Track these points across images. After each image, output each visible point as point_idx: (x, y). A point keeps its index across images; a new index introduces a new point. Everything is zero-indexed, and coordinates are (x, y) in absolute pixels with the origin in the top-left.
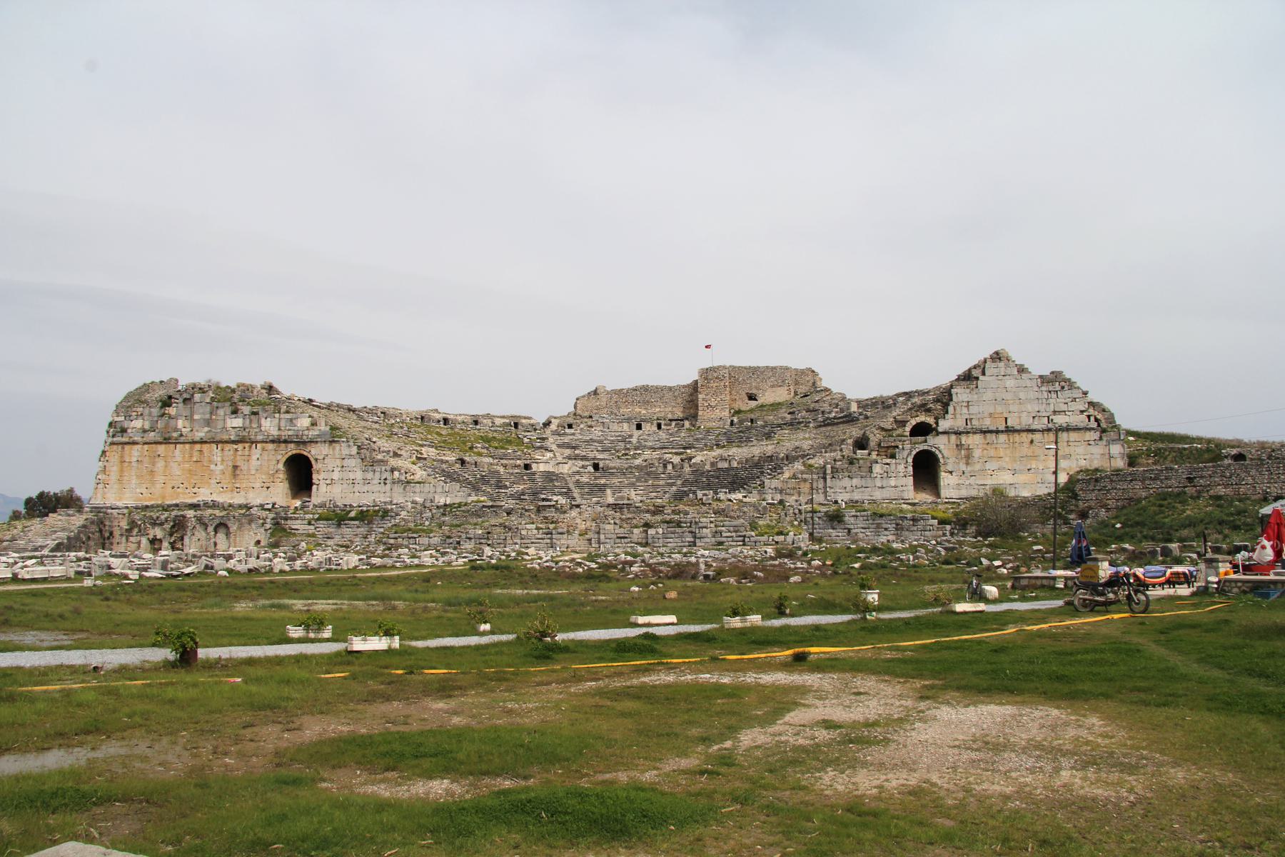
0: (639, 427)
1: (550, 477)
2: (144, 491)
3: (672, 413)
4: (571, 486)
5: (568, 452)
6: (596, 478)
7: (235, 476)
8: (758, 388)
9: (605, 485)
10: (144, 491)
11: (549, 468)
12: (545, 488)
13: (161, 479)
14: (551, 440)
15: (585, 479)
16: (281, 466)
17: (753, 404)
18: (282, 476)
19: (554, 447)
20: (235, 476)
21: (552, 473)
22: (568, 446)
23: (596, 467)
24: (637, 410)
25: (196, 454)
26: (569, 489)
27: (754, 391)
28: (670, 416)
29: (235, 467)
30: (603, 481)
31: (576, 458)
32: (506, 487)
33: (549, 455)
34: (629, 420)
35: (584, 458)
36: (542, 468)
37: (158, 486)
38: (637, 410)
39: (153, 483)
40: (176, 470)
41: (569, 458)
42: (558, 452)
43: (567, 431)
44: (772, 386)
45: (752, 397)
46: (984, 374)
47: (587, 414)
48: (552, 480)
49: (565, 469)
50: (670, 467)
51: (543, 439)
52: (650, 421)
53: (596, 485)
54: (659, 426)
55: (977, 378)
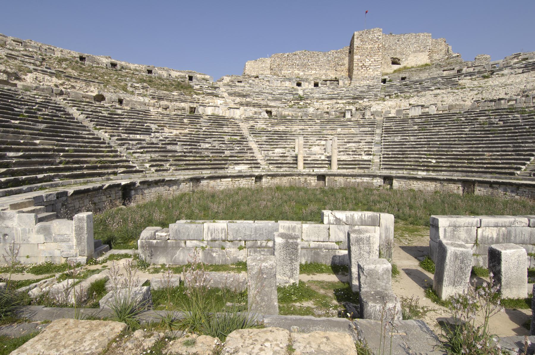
0: (299, 85)
1: (218, 121)
3: (326, 75)
4: (245, 132)
5: (238, 100)
6: (273, 125)
8: (402, 54)
9: (285, 133)
11: (220, 112)
12: (211, 136)
14: (222, 89)
15: (260, 125)
17: (396, 67)
19: (225, 95)
21: (224, 118)
22: (240, 95)
23: (269, 113)
24: (296, 72)
26: (243, 137)
27: (398, 56)
28: (324, 77)
30: (281, 128)
31: (248, 104)
32: (148, 131)
33: (219, 101)
34: (290, 80)
35: (259, 106)
36: (209, 111)
38: (296, 72)
41: (242, 104)
42: (230, 100)
43: (237, 84)
44: (415, 52)
45: (395, 62)
47: (254, 74)
48: (221, 126)
49: (238, 114)
50: (348, 116)
51: (216, 88)
52: (306, 80)
53: (276, 132)
54: (316, 85)
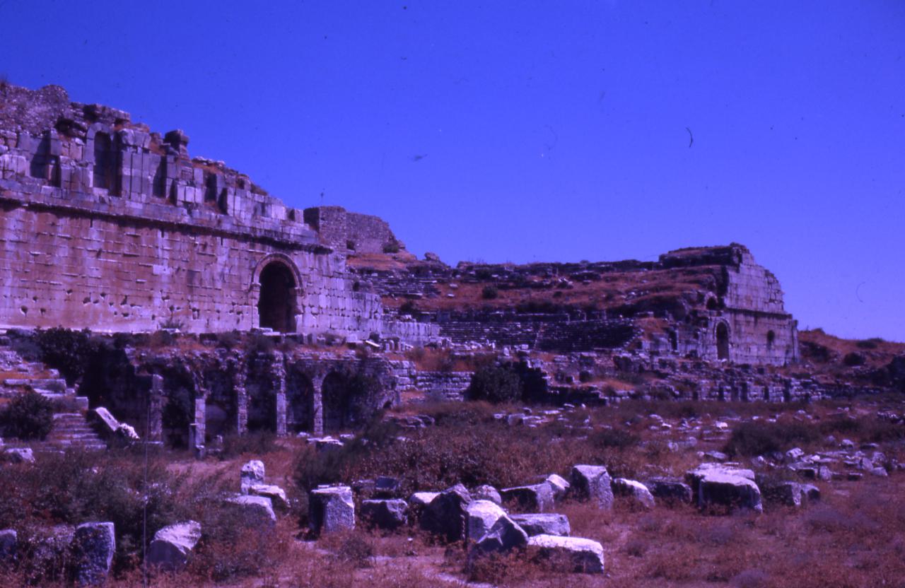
2: (30, 304)
7: (191, 289)
8: (355, 236)
10: (30, 304)
13: (61, 281)
16: (257, 281)
18: (257, 295)
20: (191, 289)
25: (128, 241)
29: (191, 274)
37: (60, 296)
39: (49, 288)
40: (93, 268)
44: (369, 237)
46: (740, 261)
55: (738, 266)
